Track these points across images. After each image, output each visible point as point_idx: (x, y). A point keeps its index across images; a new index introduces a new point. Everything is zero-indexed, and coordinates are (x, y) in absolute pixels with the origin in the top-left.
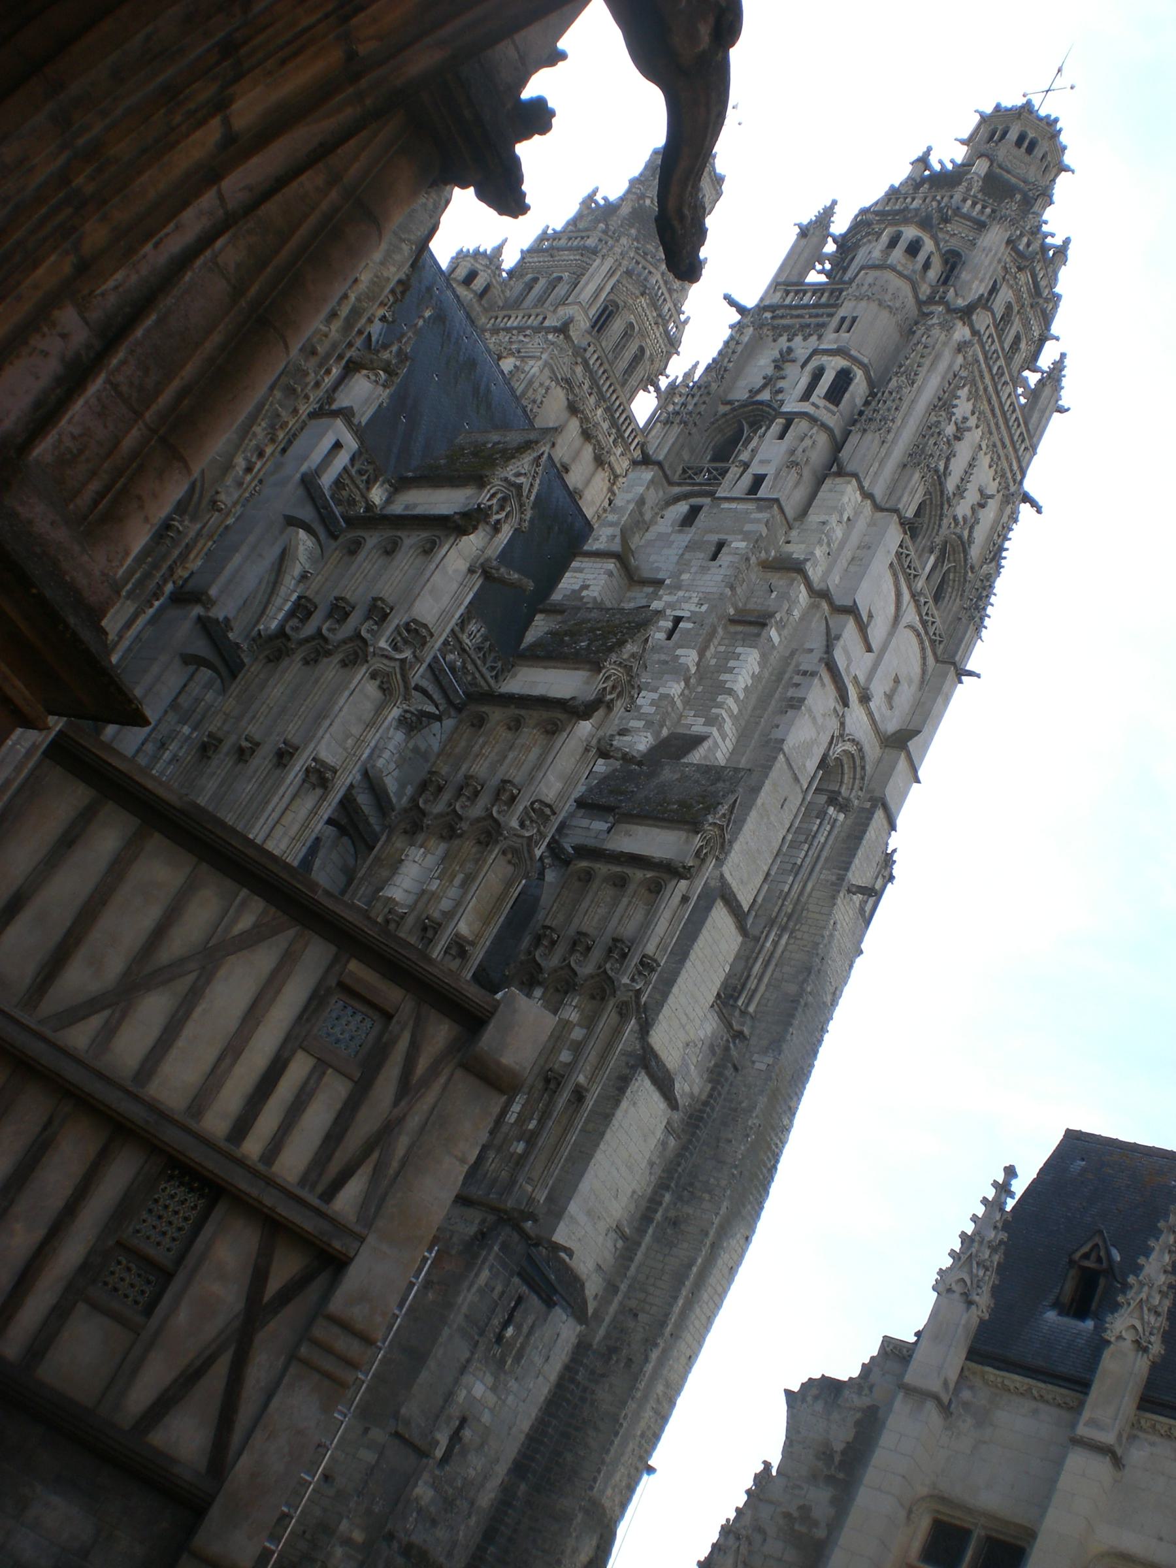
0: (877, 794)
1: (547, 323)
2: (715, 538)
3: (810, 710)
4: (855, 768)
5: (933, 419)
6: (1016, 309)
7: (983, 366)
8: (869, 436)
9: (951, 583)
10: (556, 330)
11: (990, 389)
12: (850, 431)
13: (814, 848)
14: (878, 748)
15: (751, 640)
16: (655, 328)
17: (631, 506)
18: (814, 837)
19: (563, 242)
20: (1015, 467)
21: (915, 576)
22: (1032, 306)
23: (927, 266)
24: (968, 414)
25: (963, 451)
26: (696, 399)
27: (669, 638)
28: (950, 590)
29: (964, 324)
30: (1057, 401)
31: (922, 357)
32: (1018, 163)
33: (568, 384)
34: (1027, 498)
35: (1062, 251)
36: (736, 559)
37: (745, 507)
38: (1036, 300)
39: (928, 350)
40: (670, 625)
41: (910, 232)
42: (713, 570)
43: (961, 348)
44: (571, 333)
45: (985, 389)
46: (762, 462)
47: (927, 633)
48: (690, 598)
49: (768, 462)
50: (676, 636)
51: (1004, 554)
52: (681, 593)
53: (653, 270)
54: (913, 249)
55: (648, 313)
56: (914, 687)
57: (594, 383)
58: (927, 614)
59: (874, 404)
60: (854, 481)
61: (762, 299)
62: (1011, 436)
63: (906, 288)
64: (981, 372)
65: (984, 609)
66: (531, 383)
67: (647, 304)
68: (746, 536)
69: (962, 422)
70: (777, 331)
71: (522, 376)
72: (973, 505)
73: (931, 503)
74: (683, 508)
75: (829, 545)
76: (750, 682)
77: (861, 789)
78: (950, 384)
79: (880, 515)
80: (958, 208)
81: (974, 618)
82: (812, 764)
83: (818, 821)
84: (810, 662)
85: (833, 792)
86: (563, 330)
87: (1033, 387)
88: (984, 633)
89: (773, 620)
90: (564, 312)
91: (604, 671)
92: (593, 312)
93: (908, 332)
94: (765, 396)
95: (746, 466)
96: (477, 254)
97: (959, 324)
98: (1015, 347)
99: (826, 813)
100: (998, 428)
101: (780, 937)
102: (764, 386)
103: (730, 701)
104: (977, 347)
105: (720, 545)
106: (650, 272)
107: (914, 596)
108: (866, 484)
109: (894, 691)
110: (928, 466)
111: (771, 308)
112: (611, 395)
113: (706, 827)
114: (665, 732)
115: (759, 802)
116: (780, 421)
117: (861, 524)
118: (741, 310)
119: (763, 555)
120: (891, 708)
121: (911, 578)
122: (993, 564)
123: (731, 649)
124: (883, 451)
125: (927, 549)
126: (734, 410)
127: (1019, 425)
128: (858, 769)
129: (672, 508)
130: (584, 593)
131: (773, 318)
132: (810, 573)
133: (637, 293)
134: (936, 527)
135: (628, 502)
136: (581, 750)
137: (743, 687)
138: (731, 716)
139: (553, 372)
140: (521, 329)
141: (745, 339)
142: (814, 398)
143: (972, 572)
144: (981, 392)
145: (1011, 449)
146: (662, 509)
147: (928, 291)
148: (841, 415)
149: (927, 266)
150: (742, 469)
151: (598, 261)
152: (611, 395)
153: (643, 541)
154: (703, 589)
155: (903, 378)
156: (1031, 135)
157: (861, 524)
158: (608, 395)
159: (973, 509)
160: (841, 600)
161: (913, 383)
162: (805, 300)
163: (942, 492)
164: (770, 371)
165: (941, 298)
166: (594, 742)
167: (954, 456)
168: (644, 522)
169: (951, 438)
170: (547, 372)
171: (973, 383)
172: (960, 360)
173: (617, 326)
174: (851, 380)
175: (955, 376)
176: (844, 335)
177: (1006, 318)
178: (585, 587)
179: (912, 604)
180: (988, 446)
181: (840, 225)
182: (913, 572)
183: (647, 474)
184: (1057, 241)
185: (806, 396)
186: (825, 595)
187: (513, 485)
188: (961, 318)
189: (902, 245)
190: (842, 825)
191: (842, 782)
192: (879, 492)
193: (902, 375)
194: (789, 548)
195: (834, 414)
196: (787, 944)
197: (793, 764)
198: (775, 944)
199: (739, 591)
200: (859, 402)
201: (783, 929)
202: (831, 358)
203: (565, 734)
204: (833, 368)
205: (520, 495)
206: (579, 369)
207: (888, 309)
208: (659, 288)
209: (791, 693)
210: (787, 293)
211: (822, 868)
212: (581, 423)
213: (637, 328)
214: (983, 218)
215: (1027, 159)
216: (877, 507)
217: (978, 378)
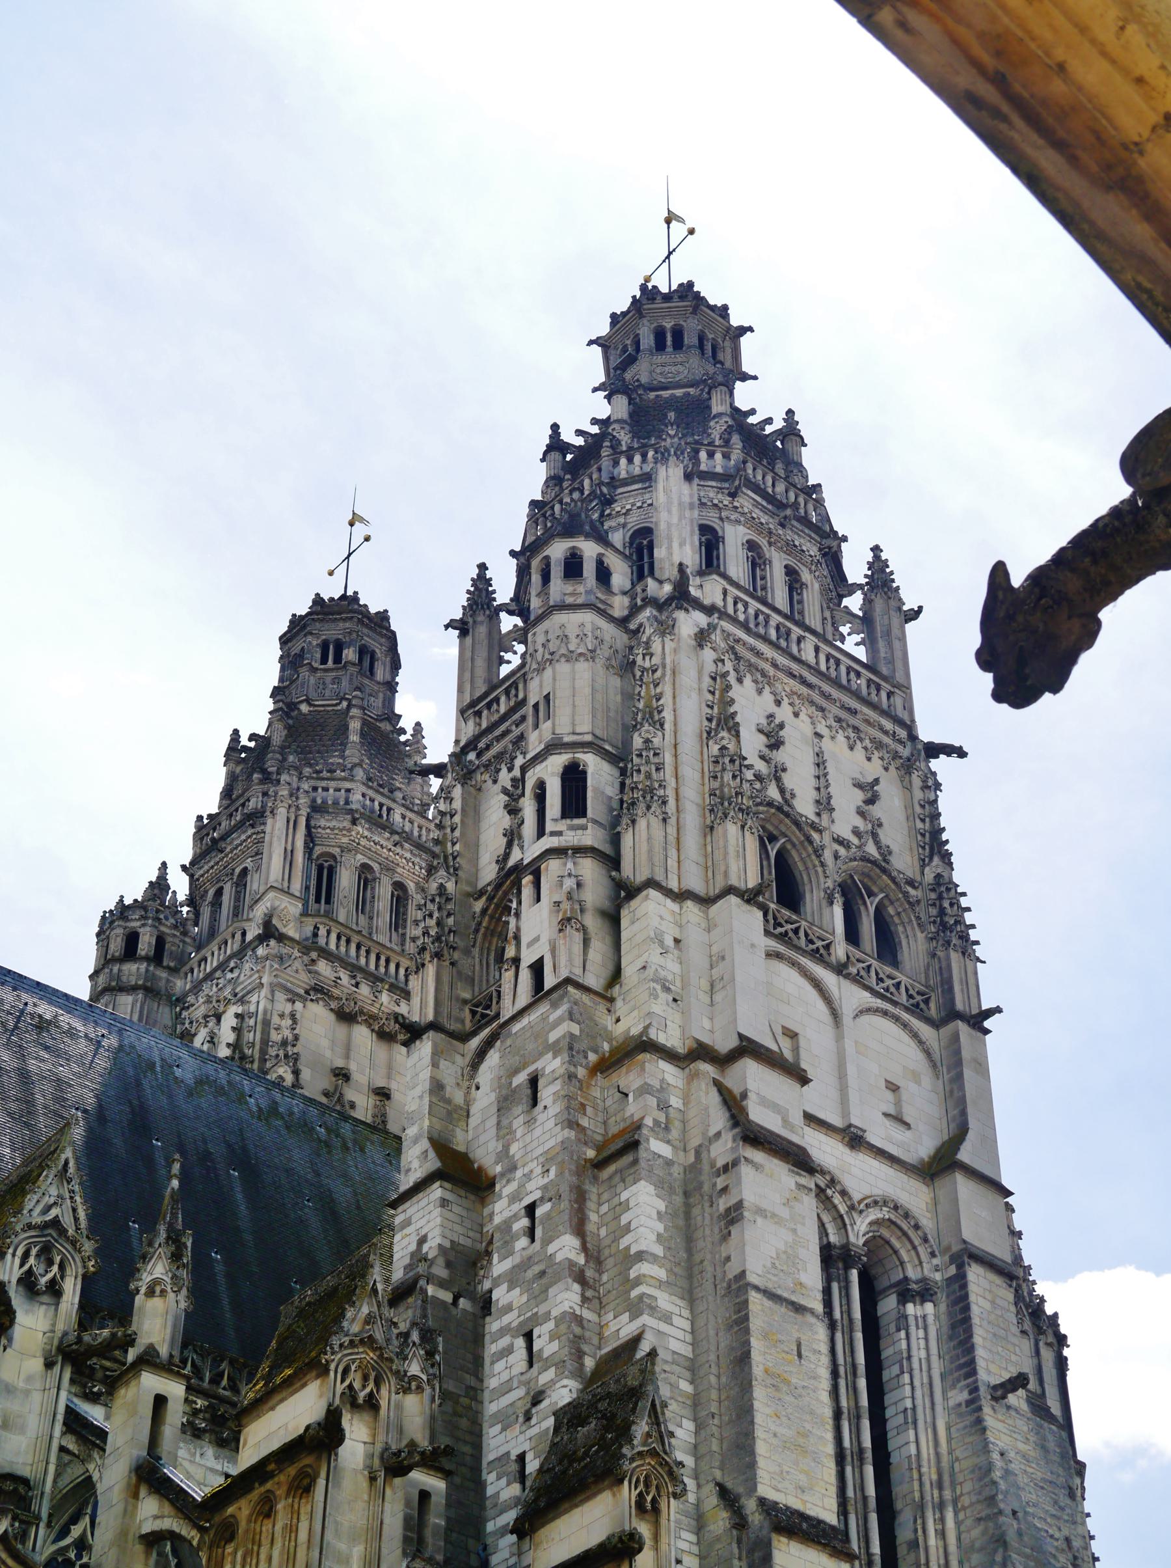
0: (956, 1248)
1: (249, 937)
2: (521, 1078)
3: (761, 1212)
4: (905, 1234)
5: (715, 749)
6: (763, 542)
7: (751, 640)
8: (642, 824)
9: (896, 920)
10: (262, 939)
11: (782, 660)
12: (619, 833)
13: (916, 1373)
14: (924, 1188)
15: (628, 1177)
16: (398, 850)
17: (426, 1099)
18: (909, 1358)
19: (225, 825)
20: (888, 725)
21: (827, 947)
22: (783, 526)
23: (603, 574)
24: (772, 708)
26: (436, 915)
27: (533, 1241)
28: (900, 929)
29: (687, 610)
30: (900, 609)
31: (656, 685)
32: (673, 369)
33: (318, 991)
34: (934, 750)
35: (791, 431)
36: (557, 1086)
37: (538, 1013)
38: (782, 514)
39: (658, 674)
40: (525, 1222)
41: (557, 550)
42: (541, 1118)
43: (702, 637)
44: (284, 930)
45: (775, 665)
46: (529, 945)
47: (895, 1003)
48: (531, 1171)
49: (537, 939)
50: (539, 1232)
51: (944, 837)
52: (519, 1174)
53: (348, 785)
54: (573, 566)
55: (376, 838)
56: (927, 1079)
57: (354, 969)
58: (880, 980)
59: (628, 782)
60: (652, 893)
61: (457, 742)
62: (856, 695)
63: (588, 618)
64: (752, 649)
65: (960, 921)
66: (266, 1023)
67: (369, 829)
68: (555, 1049)
69: (769, 724)
70: (492, 767)
71: (252, 1022)
72: (858, 808)
73: (794, 845)
75: (667, 990)
76: (660, 1227)
77: (933, 1255)
78: (713, 693)
79: (715, 909)
80: (612, 478)
81: (949, 943)
82: (812, 1275)
83: (903, 1334)
84: (721, 1151)
85: (899, 1283)
86: (269, 932)
87: (860, 614)
88: (979, 951)
89: (645, 1131)
90: (260, 911)
91: (332, 1366)
92: (297, 887)
93: (627, 667)
95: (516, 961)
97: (680, 615)
98: (798, 586)
99: (906, 1317)
100: (827, 697)
101: (942, 1520)
102: (509, 845)
103: (644, 1268)
104: (724, 624)
105: (534, 1081)
106: (348, 791)
107: (840, 969)
108: (673, 884)
109: (898, 1103)
110: (741, 810)
111: (471, 745)
112: (387, 967)
113: (627, 1466)
114: (589, 1363)
115: (757, 1370)
116: (527, 880)
117: (695, 936)
119: (592, 1057)
120: (907, 1125)
121: (820, 955)
122: (936, 860)
123: (616, 1201)
124: (672, 830)
125: (824, 903)
126: (490, 899)
127: (858, 675)
128: (911, 1233)
129: (484, 1067)
130: (425, 1248)
131: (479, 756)
132: (662, 1039)
133: (347, 824)
134: (820, 869)
135: (421, 1097)
136: (365, 1484)
137: (654, 1238)
138: (660, 1284)
139: (288, 990)
140: (222, 966)
141: (457, 804)
142: (549, 827)
143: (914, 887)
144: (771, 671)
145: (866, 710)
146: (472, 1077)
147: (626, 601)
148: (595, 822)
150: (513, 968)
151: (269, 821)
152: (387, 967)
153: (470, 1132)
154: (540, 1150)
155: (646, 727)
156: (668, 325)
157: (695, 936)
158: (382, 970)
159: (861, 813)
160: (724, 1044)
161: (662, 725)
162: (503, 709)
163: (797, 824)
164: (506, 821)
165: (643, 600)
166: (377, 1462)
167: (784, 770)
168: (458, 1108)
169: (766, 751)
170: (280, 996)
171: (751, 667)
172: (708, 655)
173: (346, 880)
174: (584, 773)
175: (714, 679)
176: (546, 726)
178: (422, 1240)
179: (846, 985)
180: (830, 727)
181: (504, 589)
182: (819, 944)
183: (425, 1047)
184: (778, 424)
185: (541, 832)
186: (701, 1052)
187: (46, 1225)
188: (679, 607)
189: (557, 572)
190: (937, 1317)
191: (902, 1263)
192: (695, 882)
193: (642, 725)
194: (619, 1030)
195: (584, 828)
196: (958, 1523)
197: (779, 1292)
198: (942, 1534)
199: (584, 1122)
200: (612, 791)
201: (941, 1506)
202: (544, 764)
203: (321, 1482)
204: (553, 774)
205: (62, 1232)
206: (323, 967)
207: (582, 659)
208: (372, 800)
209: (723, 1204)
210: (478, 714)
211: (944, 1392)
212: (370, 1026)
213: (376, 866)
214: (647, 468)
215: (680, 357)
216: (706, 901)
217: (754, 660)
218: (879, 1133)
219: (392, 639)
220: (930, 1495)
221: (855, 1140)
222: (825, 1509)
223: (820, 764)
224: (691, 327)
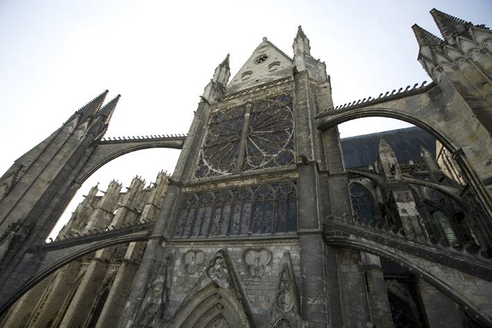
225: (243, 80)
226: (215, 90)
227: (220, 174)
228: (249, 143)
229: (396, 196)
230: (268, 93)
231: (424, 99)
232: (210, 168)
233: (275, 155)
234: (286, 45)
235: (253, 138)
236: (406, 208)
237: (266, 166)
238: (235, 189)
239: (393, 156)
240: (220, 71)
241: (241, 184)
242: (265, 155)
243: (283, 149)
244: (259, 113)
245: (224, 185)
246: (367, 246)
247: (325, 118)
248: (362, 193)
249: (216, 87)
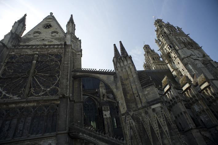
23: (164, 35)
25: (181, 39)
33: (157, 64)
34: (188, 35)
35: (168, 23)
43: (173, 35)
74: (173, 63)
94: (168, 52)
96: (144, 65)
105: (178, 63)
118: (159, 50)
121: (190, 48)
149: (164, 35)
173: (155, 58)
177: (172, 30)
185: (170, 50)
192: (181, 48)
216: (182, 49)
218: (199, 56)
219: (149, 46)
220: (216, 75)
221: (199, 57)
222: (213, 78)
223: (182, 39)
224: (159, 21)
225: (34, 36)
226: (13, 39)
227: (11, 98)
228: (34, 80)
229: (103, 109)
230: (49, 51)
231: (112, 78)
232: (4, 93)
233: (49, 89)
234: (63, 24)
235: (36, 77)
236: (106, 114)
237: (43, 95)
238: (21, 109)
239: (105, 89)
240: (19, 25)
241: (26, 105)
242: (42, 89)
243: (53, 86)
244: (42, 62)
245: (14, 106)
246: (86, 138)
247: (77, 73)
248: (92, 103)
249: (14, 36)
